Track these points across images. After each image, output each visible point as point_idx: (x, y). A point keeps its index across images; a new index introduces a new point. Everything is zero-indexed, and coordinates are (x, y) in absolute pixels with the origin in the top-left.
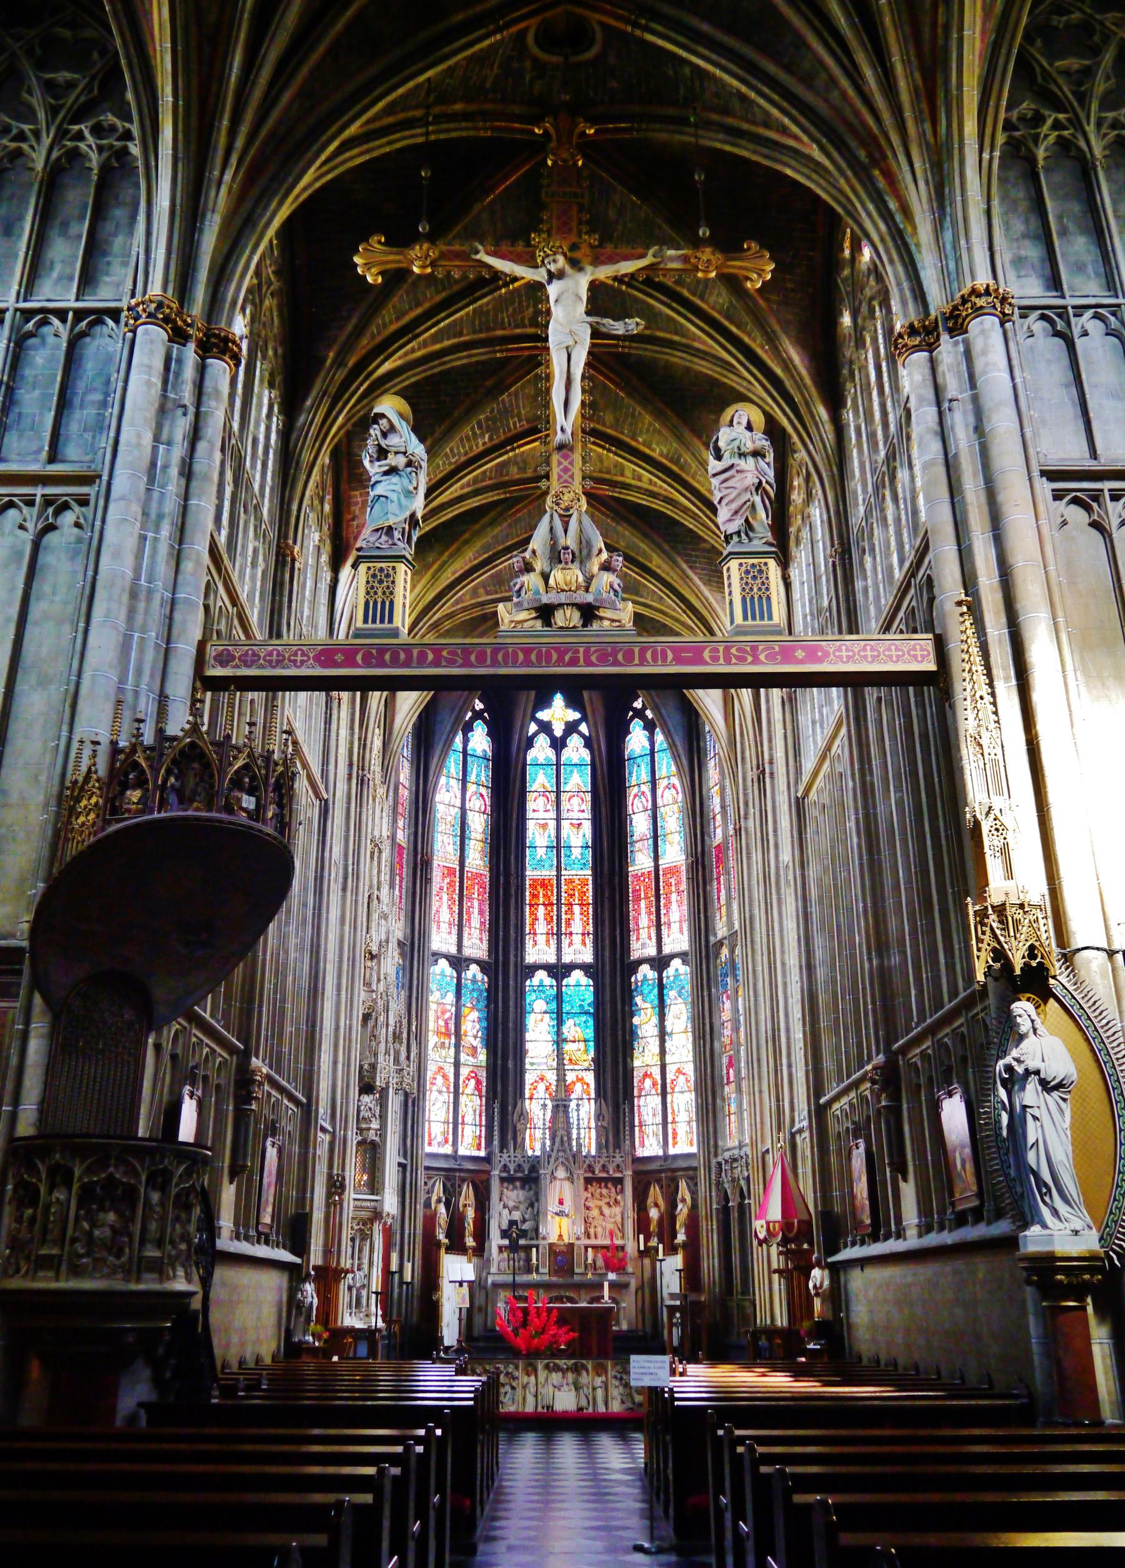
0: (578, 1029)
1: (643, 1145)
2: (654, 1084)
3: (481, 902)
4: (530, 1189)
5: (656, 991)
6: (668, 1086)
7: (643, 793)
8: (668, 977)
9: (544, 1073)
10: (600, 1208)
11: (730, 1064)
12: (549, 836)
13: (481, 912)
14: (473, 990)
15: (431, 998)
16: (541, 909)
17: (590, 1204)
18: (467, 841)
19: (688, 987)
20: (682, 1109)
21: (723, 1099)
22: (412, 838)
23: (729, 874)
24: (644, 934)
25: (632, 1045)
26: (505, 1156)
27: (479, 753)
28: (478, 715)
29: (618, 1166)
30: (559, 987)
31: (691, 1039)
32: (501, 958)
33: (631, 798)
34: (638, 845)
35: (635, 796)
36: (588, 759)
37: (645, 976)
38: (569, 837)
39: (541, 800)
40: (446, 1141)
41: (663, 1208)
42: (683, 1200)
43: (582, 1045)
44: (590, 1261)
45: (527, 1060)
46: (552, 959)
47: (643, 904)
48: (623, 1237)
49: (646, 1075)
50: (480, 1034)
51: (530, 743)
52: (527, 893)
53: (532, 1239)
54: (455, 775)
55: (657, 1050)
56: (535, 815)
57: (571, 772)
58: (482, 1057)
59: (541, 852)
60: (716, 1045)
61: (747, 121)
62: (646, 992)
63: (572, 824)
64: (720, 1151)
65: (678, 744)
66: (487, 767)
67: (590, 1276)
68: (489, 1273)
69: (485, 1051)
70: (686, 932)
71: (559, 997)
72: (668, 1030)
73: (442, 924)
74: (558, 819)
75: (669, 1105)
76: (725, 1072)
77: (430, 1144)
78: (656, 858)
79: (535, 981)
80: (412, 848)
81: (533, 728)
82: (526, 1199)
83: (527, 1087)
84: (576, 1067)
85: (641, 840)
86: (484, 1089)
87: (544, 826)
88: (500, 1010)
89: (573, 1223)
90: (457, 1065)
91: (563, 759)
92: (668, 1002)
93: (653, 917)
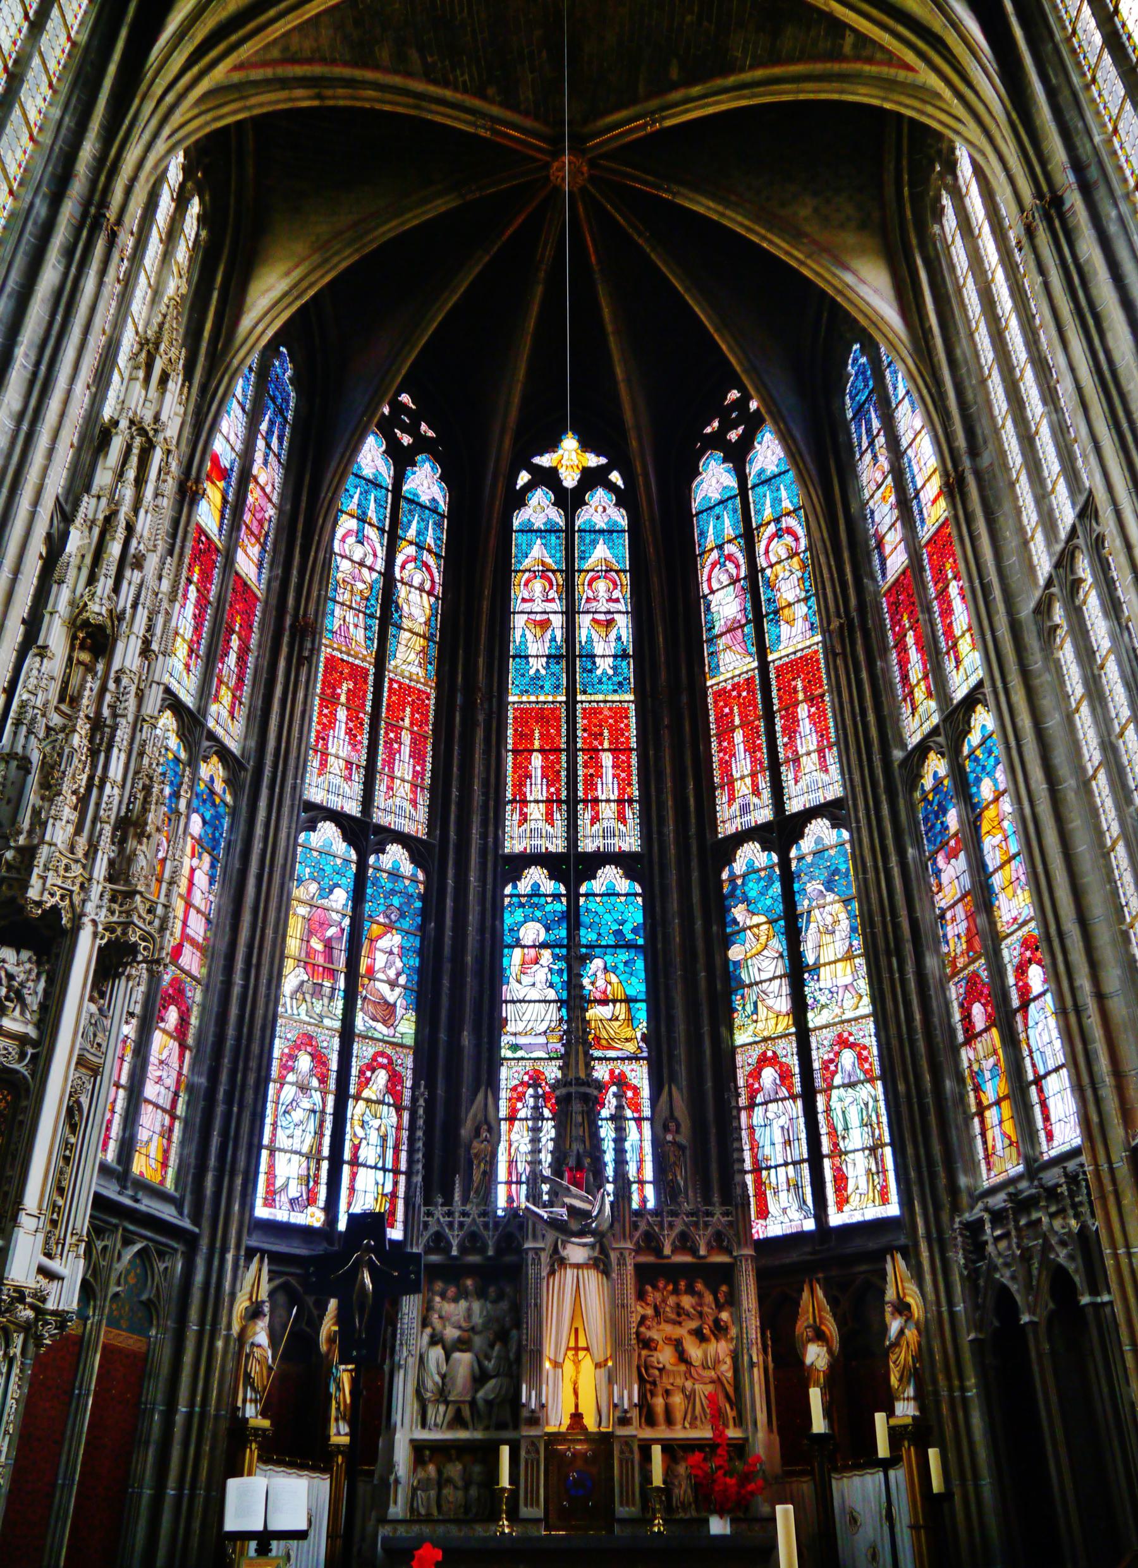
0: (614, 979)
1: (764, 1213)
2: (785, 1076)
3: (417, 741)
4: (500, 1297)
5: (777, 888)
6: (817, 1075)
7: (730, 557)
8: (801, 858)
9: (540, 1066)
10: (678, 1345)
11: (973, 991)
12: (553, 639)
13: (417, 755)
14: (393, 892)
15: (298, 892)
16: (537, 760)
17: (654, 1335)
18: (392, 630)
19: (845, 865)
20: (854, 1120)
21: (960, 1079)
22: (276, 585)
23: (929, 610)
24: (743, 788)
25: (731, 1002)
26: (439, 1211)
27: (424, 499)
28: (421, 445)
29: (719, 1236)
30: (573, 896)
31: (863, 971)
32: (452, 835)
33: (706, 570)
34: (722, 642)
35: (714, 565)
36: (624, 523)
37: (750, 864)
38: (590, 641)
39: (538, 586)
40: (311, 1200)
41: (836, 1346)
42: (902, 1308)
43: (621, 1009)
44: (658, 1480)
45: (505, 1039)
46: (557, 845)
47: (738, 736)
48: (739, 1422)
49: (764, 1061)
50: (402, 980)
51: (519, 500)
52: (510, 732)
53: (501, 1426)
54: (375, 521)
55: (784, 1004)
56: (527, 606)
57: (594, 543)
58: (406, 1027)
59: (537, 665)
60: (931, 962)
62: (752, 894)
63: (594, 620)
64: (965, 1200)
65: (798, 436)
66: (438, 525)
67: (658, 1526)
68: (383, 1520)
69: (411, 1016)
70: (834, 769)
71: (572, 918)
72: (810, 959)
73: (331, 759)
74: (570, 614)
75: (821, 1118)
76: (957, 1016)
77: (269, 1202)
78: (762, 652)
79: (524, 886)
80: (273, 601)
81: (524, 477)
82: (489, 1320)
83: (504, 1094)
84: (612, 1054)
85: (729, 631)
86: (407, 1094)
87: (545, 625)
88: (448, 933)
89: (610, 1381)
90: (347, 1034)
91: (578, 523)
92: (803, 905)
93: (763, 755)
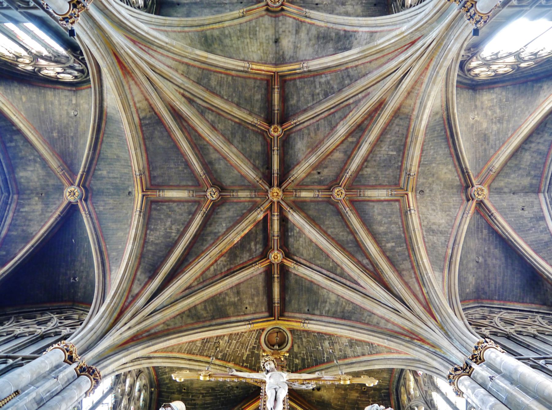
61: (355, 357)
